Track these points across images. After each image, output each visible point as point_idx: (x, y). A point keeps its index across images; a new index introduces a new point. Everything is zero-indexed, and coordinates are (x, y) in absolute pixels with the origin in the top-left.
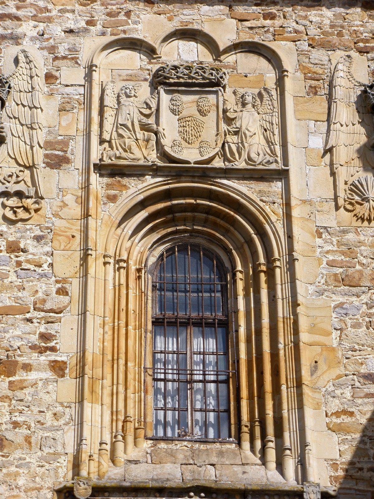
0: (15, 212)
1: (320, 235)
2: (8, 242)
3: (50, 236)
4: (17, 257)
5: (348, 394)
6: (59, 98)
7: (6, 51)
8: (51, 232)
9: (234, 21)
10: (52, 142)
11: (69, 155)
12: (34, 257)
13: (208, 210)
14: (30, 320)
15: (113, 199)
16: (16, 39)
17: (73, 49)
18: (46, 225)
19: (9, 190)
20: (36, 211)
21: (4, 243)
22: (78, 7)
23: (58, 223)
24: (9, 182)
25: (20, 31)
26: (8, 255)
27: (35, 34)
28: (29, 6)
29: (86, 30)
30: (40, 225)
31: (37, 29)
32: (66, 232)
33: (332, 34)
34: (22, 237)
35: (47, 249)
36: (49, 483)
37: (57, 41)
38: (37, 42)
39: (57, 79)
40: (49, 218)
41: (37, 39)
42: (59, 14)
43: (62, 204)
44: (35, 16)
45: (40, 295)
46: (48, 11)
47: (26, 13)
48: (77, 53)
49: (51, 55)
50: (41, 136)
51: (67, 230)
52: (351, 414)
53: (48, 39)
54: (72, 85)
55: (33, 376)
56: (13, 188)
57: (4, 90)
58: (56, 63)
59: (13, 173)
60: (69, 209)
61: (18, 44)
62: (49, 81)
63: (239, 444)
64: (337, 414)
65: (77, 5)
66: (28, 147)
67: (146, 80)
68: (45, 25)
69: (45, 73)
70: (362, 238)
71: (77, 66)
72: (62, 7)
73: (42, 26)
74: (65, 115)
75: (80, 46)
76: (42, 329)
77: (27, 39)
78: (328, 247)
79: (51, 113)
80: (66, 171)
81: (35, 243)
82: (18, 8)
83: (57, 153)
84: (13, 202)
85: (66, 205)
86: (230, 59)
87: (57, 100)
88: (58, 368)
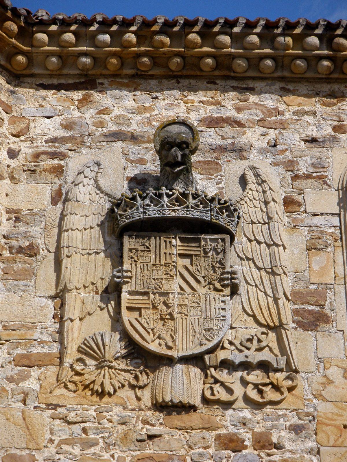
0: (261, 392)
2: (254, 434)
3: (313, 426)
4: (269, 455)
6: (306, 232)
7: (227, 168)
8: (314, 419)
10: (303, 293)
11: (327, 311)
12: (293, 456)
16: (240, 152)
17: (319, 165)
18: (306, 410)
19: (250, 359)
20: (291, 389)
21: (249, 435)
23: (322, 407)
24: (248, 349)
25: (243, 140)
26: (256, 452)
27: (265, 145)
28: (254, 106)
29: (334, 139)
30: (296, 410)
31: (267, 138)
32: (335, 420)
34: (273, 427)
35: (311, 444)
37: (296, 153)
38: (269, 155)
39: (300, 205)
40: (309, 400)
41: (269, 151)
42: (295, 117)
43: (324, 380)
44: (262, 120)
46: (280, 113)
47: (250, 116)
48: (325, 170)
49: (289, 173)
50: (287, 284)
51: (336, 417)
53: (283, 151)
54: (322, 214)
56: (255, 357)
57: (233, 221)
58: (297, 183)
59: (252, 336)
60: (336, 387)
62: (290, 209)
65: (318, 106)
66: (271, 300)
68: (277, 132)
69: (283, 197)
71: (325, 187)
72: (299, 108)
73: (272, 134)
74: (317, 255)
75: (328, 160)
77: (255, 151)
79: (296, 253)
80: (326, 333)
81: (293, 436)
82: (239, 110)
83: (310, 308)
85: (330, 382)
87: (302, 236)
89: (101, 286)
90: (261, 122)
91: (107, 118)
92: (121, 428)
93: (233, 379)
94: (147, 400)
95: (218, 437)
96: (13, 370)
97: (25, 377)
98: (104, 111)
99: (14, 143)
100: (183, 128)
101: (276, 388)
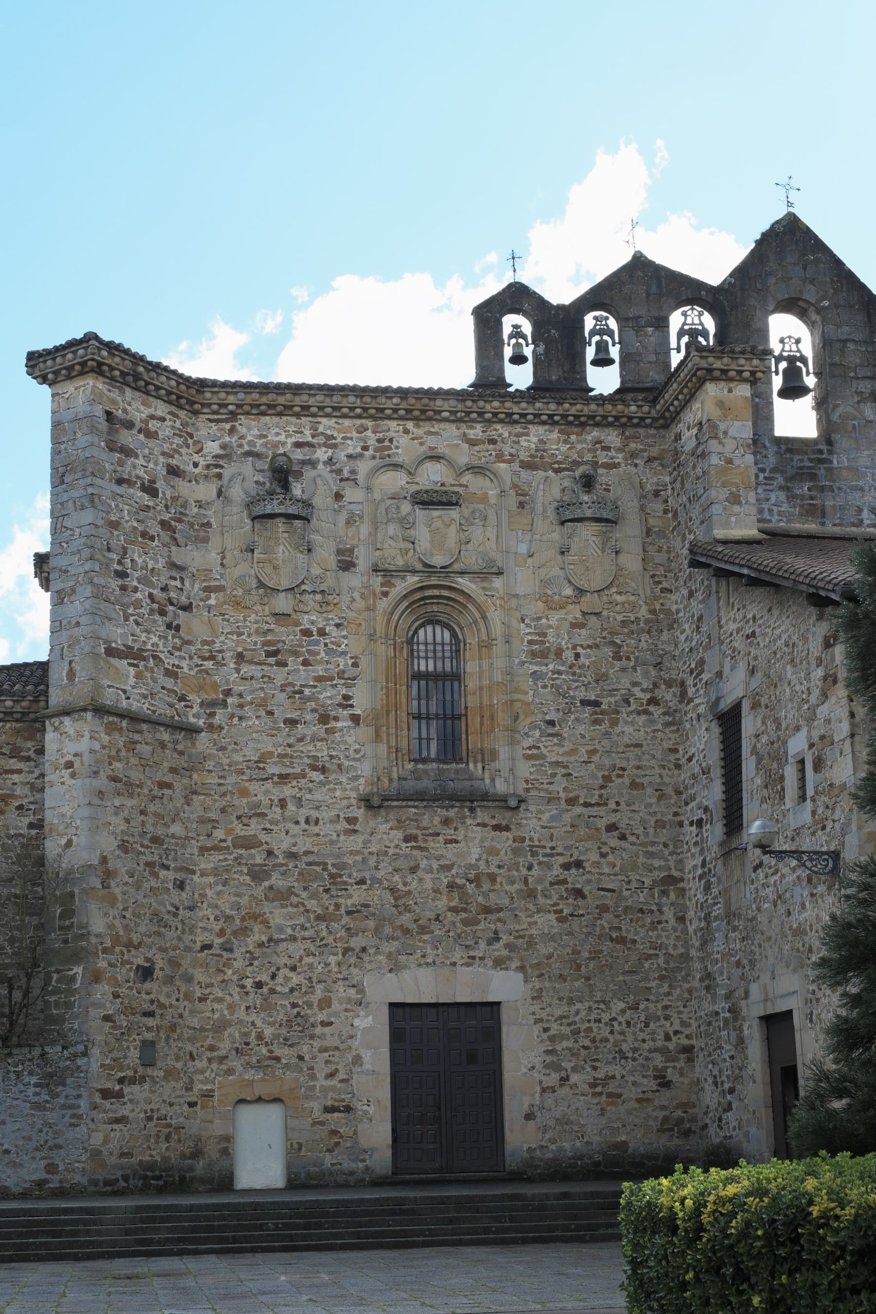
1: (523, 621)
5: (537, 733)
9: (467, 446)
13: (448, 598)
14: (336, 685)
15: (385, 594)
16: (313, 464)
22: (355, 434)
29: (361, 456)
33: (536, 457)
35: (344, 633)
36: (353, 794)
45: (341, 667)
46: (335, 438)
52: (538, 748)
55: (339, 724)
61: (315, 468)
63: (467, 763)
64: (530, 748)
67: (405, 498)
70: (551, 623)
76: (344, 692)
78: (528, 631)
82: (313, 437)
84: (318, 597)
86: (464, 480)
88: (355, 719)
89: (244, 548)
90: (325, 445)
91: (244, 442)
92: (255, 626)
93: (307, 597)
94: (267, 612)
95: (301, 630)
96: (203, 595)
97: (209, 598)
98: (242, 437)
99: (196, 458)
100: (285, 459)
101: (328, 604)
